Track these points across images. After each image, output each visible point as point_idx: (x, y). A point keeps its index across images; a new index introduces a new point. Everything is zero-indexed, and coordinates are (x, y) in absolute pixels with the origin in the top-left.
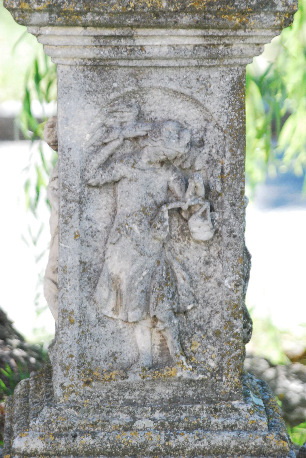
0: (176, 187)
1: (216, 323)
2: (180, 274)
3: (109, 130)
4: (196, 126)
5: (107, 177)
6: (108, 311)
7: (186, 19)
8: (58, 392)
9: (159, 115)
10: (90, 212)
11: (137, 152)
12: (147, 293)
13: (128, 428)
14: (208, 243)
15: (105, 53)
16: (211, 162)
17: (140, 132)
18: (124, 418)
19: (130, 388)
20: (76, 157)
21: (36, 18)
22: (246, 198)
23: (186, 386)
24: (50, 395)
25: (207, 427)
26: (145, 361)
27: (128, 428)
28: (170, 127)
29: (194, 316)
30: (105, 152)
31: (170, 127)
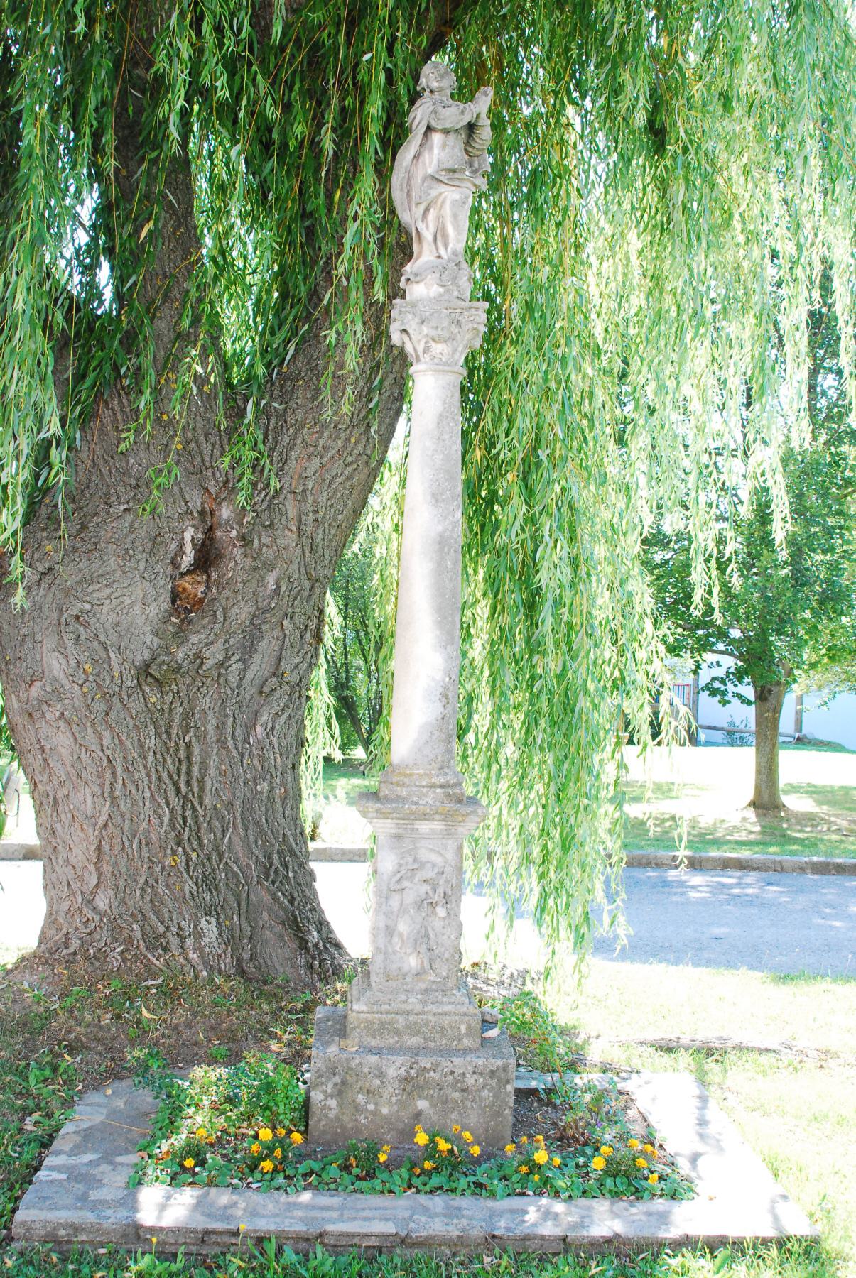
0: (431, 893)
1: (447, 955)
2: (431, 933)
3: (401, 865)
4: (440, 865)
5: (399, 887)
6: (397, 948)
7: (438, 817)
8: (373, 984)
9: (424, 860)
10: (391, 902)
11: (413, 877)
12: (416, 941)
13: (405, 1002)
14: (444, 919)
15: (400, 831)
16: (447, 881)
17: (415, 867)
18: (403, 997)
19: (406, 984)
20: (385, 877)
21: (370, 815)
22: (565, 1032)
23: (219, 593)
24: (370, 986)
25: (441, 1003)
26: (414, 972)
27: (405, 1002)
28: (429, 865)
29: (436, 951)
30: (398, 876)
31: (429, 865)
